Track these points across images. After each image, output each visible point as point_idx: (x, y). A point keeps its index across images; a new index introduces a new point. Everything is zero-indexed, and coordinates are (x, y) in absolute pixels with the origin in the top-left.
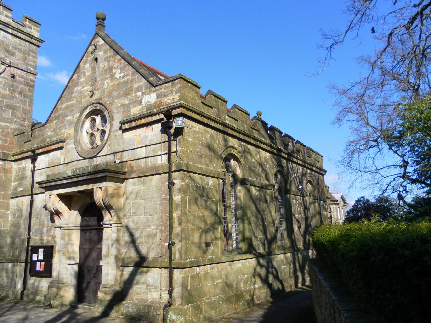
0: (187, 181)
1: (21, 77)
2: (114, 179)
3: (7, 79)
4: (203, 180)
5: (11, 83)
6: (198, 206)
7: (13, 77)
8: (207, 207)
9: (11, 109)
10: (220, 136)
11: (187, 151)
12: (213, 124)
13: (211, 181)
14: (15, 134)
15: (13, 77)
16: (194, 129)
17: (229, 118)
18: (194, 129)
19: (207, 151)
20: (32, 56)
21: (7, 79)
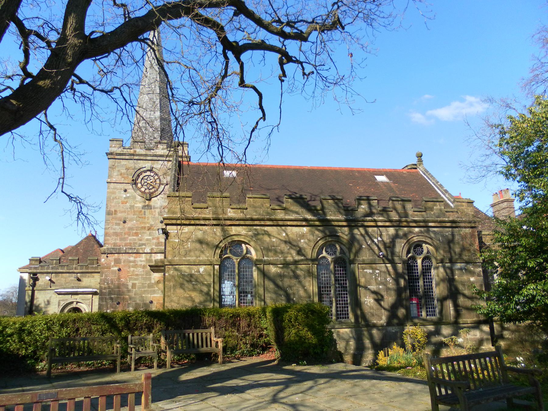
0: (172, 272)
2: (160, 271)
6: (184, 289)
8: (194, 290)
10: (218, 230)
13: (202, 269)
17: (232, 211)
19: (198, 245)
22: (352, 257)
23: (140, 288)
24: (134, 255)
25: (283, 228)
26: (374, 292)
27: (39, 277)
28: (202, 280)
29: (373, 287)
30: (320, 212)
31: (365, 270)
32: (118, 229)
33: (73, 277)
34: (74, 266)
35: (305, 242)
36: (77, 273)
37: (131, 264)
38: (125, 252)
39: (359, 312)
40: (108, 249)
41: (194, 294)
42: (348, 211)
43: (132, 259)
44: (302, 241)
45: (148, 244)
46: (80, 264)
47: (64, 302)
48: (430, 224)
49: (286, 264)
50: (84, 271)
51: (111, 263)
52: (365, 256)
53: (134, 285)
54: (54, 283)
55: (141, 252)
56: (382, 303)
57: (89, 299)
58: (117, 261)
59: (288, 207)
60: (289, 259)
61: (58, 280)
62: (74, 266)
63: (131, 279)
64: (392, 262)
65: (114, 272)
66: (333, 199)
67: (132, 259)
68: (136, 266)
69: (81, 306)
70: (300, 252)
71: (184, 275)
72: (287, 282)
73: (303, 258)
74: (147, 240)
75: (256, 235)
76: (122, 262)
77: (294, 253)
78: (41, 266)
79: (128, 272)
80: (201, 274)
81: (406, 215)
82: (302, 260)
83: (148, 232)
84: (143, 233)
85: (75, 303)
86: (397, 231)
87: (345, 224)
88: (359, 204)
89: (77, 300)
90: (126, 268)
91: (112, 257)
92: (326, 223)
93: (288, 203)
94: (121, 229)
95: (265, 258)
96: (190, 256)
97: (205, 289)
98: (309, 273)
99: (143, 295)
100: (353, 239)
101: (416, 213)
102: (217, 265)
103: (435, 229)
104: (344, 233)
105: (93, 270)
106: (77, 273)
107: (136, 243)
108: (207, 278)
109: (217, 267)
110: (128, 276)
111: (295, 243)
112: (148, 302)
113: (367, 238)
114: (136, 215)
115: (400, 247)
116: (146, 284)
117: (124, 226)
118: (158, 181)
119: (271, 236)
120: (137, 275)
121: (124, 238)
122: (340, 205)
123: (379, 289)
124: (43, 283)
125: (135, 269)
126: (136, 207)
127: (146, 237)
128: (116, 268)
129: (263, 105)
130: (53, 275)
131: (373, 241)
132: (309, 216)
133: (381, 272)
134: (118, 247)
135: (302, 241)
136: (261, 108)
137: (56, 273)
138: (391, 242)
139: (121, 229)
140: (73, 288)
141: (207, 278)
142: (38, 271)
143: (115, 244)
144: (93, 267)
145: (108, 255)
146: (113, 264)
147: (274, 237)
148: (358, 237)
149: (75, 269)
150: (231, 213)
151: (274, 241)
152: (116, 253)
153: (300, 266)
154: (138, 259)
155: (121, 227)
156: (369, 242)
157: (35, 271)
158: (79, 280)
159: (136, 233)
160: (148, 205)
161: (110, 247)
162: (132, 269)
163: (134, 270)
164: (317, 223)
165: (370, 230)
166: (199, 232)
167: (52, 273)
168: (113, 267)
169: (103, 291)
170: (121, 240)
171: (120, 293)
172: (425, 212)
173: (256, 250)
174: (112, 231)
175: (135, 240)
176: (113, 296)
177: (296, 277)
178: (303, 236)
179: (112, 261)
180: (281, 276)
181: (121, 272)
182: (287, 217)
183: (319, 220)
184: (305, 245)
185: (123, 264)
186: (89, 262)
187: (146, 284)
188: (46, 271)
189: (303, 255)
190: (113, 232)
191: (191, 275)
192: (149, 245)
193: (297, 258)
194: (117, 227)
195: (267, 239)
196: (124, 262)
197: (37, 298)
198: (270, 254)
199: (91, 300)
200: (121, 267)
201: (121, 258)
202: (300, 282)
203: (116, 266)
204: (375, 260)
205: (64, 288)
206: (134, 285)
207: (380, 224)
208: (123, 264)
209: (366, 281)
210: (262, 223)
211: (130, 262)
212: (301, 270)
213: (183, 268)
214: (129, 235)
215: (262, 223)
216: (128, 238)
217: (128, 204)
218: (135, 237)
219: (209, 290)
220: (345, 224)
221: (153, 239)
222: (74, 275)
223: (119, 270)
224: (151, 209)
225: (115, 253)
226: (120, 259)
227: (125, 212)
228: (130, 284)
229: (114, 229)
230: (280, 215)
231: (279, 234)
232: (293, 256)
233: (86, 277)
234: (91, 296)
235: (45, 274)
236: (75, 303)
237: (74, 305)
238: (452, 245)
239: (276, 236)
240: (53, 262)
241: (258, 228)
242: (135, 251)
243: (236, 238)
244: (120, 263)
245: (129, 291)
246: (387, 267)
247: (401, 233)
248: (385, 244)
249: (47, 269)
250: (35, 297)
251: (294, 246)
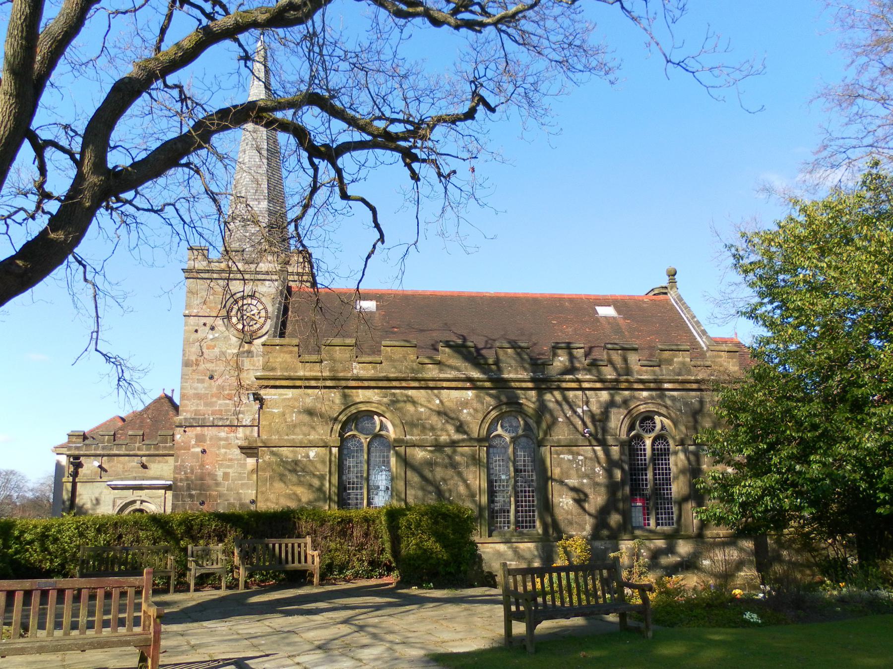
0: (268, 457)
4: (295, 453)
6: (285, 483)
8: (300, 483)
11: (270, 424)
12: (313, 383)
13: (312, 453)
16: (285, 397)
17: (358, 366)
18: (285, 397)
19: (306, 418)
22: (541, 435)
23: (236, 480)
24: (226, 428)
25: (436, 391)
26: (574, 489)
27: (83, 462)
28: (312, 469)
29: (573, 482)
30: (493, 367)
31: (562, 456)
32: (201, 388)
33: (134, 463)
34: (137, 445)
35: (469, 413)
36: (142, 456)
37: (222, 443)
38: (211, 424)
39: (549, 520)
40: (186, 419)
41: (299, 490)
42: (537, 365)
43: (223, 434)
44: (465, 411)
45: (247, 411)
46: (146, 442)
47: (121, 501)
48: (666, 386)
49: (438, 447)
50: (152, 452)
52: (561, 433)
53: (226, 476)
54: (106, 471)
56: (586, 506)
57: (160, 497)
58: (200, 439)
59: (444, 360)
60: (444, 438)
61: (112, 467)
62: (137, 445)
63: (221, 466)
64: (603, 443)
65: (194, 455)
66: (513, 347)
67: (223, 434)
68: (228, 446)
69: (147, 507)
70: (460, 428)
71: (287, 462)
72: (439, 473)
73: (465, 437)
75: (394, 402)
76: (208, 439)
77: (451, 429)
78: (86, 445)
79: (217, 455)
80: (310, 460)
81: (628, 371)
82: (463, 440)
85: (138, 502)
86: (612, 396)
87: (530, 385)
88: (555, 355)
89: (142, 498)
90: (214, 450)
91: (192, 433)
92: (500, 384)
93: (445, 355)
94: (206, 389)
95: (408, 437)
96: (294, 434)
97: (316, 483)
98: (475, 460)
99: (241, 491)
100: (542, 408)
101: (644, 368)
102: (336, 447)
103: (675, 393)
104: (529, 400)
105: (167, 452)
106: (142, 456)
107: (229, 411)
108: (319, 466)
109: (335, 450)
110: (217, 461)
111: (452, 415)
112: (248, 501)
113: (566, 407)
115: (617, 421)
116: (245, 473)
117: (210, 384)
118: (263, 313)
119: (418, 404)
120: (231, 460)
122: (526, 357)
123: (583, 484)
124: (89, 472)
125: (228, 451)
128: (199, 450)
129: (379, 221)
130: (105, 458)
131: (575, 412)
132: (476, 374)
133: (586, 458)
134: (201, 417)
135: (465, 411)
136: (377, 226)
137: (108, 455)
138: (602, 413)
140: (135, 479)
141: (319, 466)
142: (82, 452)
143: (196, 412)
144: (165, 447)
145: (187, 429)
146: (193, 442)
147: (422, 405)
148: (552, 405)
149: (139, 449)
150: (358, 370)
151: (422, 412)
152: (199, 426)
153: (459, 449)
155: (206, 385)
156: (569, 413)
157: (77, 452)
158: (144, 467)
159: (228, 395)
160: (249, 352)
161: (189, 416)
162: (223, 451)
163: (226, 453)
164: (488, 384)
165: (571, 394)
166: (310, 398)
167: (103, 456)
168: (193, 447)
169: (179, 484)
170: (206, 405)
171: (203, 488)
172: (659, 366)
173: (394, 425)
174: (192, 392)
175: (227, 405)
176: (194, 492)
177: (454, 465)
178: (465, 404)
179: (192, 438)
180: (430, 464)
181: (205, 456)
182: (442, 376)
183: (490, 380)
184: (469, 418)
185: (208, 442)
186: (159, 438)
187: (245, 473)
188: (93, 452)
189: (465, 433)
190: (194, 394)
191: (296, 462)
192: (249, 413)
193: (457, 437)
194: (199, 385)
195: (410, 408)
196: (211, 439)
197: (80, 495)
198: (415, 431)
199: (163, 498)
200: (205, 448)
201: (206, 433)
202: (460, 474)
203: (198, 446)
204: (577, 440)
205: (122, 479)
206: (226, 476)
207: (586, 385)
208: (208, 442)
209: (562, 473)
210: (404, 384)
211: (220, 439)
212: (462, 455)
213: (285, 451)
214: (219, 398)
215: (404, 384)
216: (216, 402)
217: (217, 350)
218: (228, 402)
219: (322, 485)
220: (530, 385)
222: (136, 458)
223: (204, 452)
224: (253, 357)
225: (196, 426)
226: (204, 435)
228: (220, 473)
229: (195, 389)
230: (432, 372)
231: (429, 402)
232: (450, 433)
233: (154, 462)
234: (163, 491)
235: (92, 458)
236: (138, 502)
237: (137, 506)
238: (699, 418)
239: (426, 403)
240: (104, 439)
241: (398, 391)
242: (228, 423)
243: (363, 408)
244: (204, 441)
245: (218, 484)
246: (594, 451)
247: (618, 399)
248: (593, 417)
249: (95, 450)
250: (77, 493)
251: (452, 419)
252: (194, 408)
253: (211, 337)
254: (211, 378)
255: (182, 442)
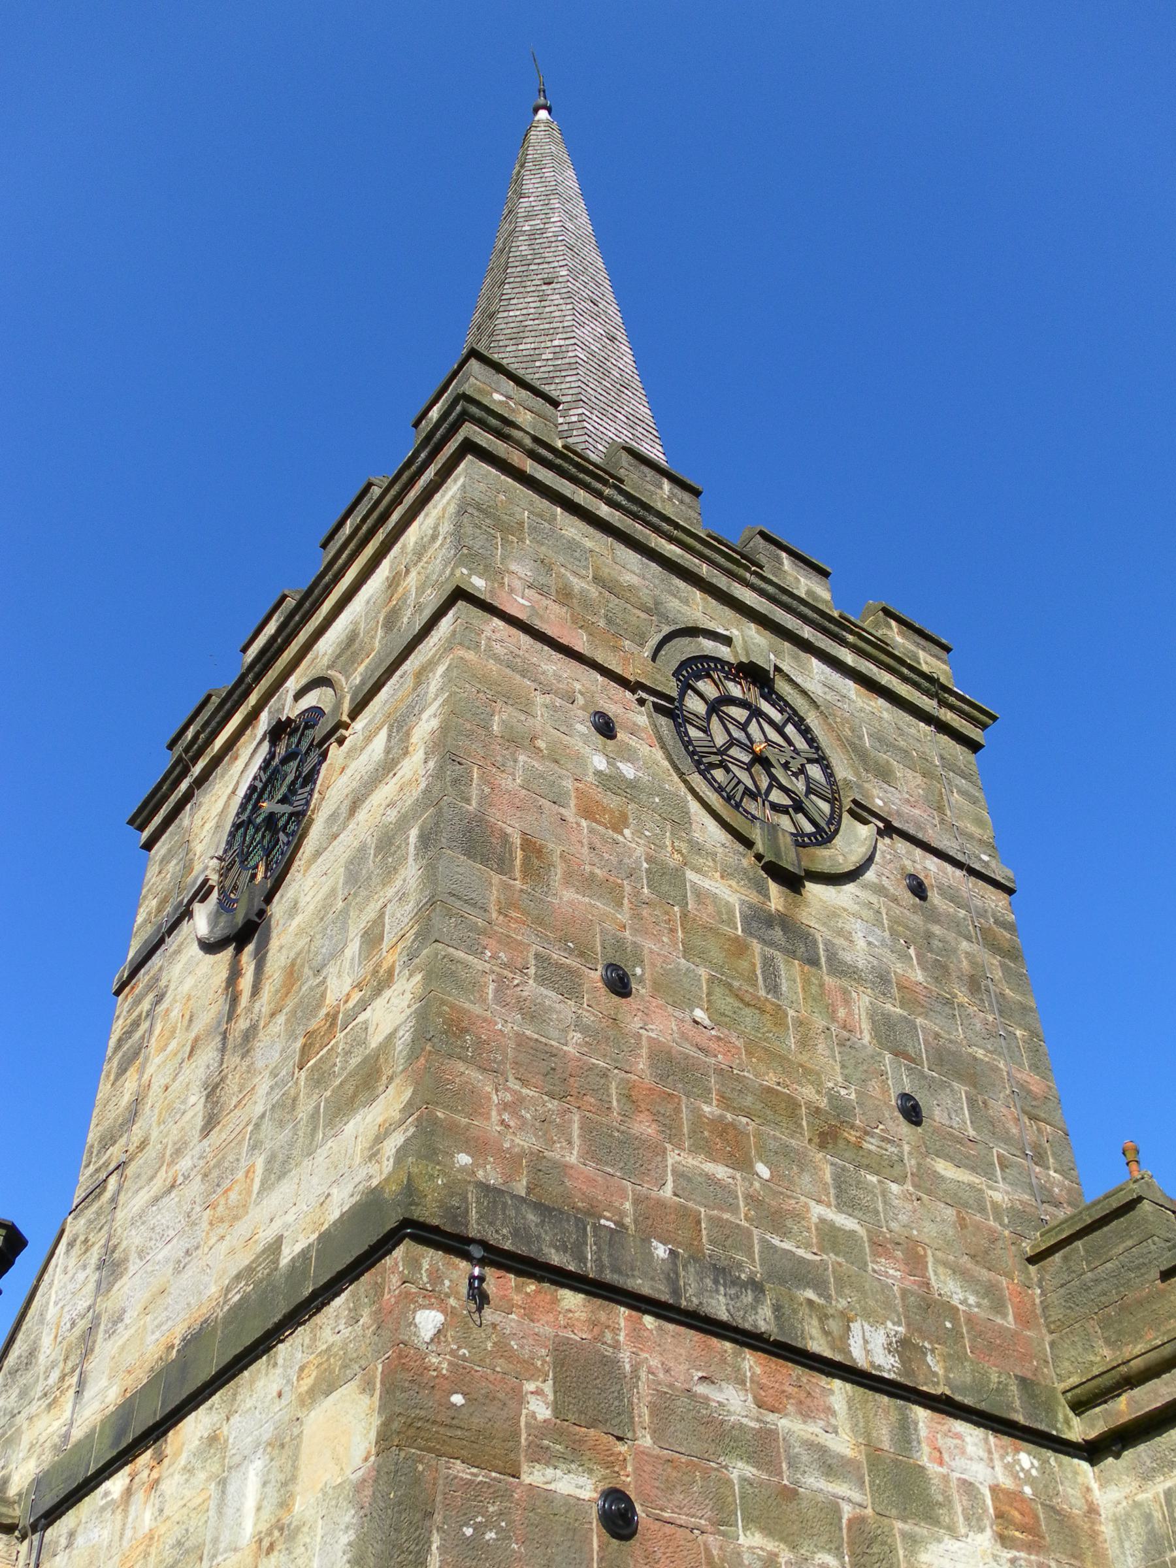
1: (945, 892)
3: (895, 900)
5: (917, 920)
7: (918, 889)
9: (960, 1077)
14: (1028, 1248)
15: (918, 889)
20: (960, 792)
21: (895, 900)
51: (520, 1398)
55: (818, 1346)
74: (831, 1237)
76: (643, 1414)
83: (825, 1166)
84: (785, 1151)
114: (702, 956)
121: (629, 1141)
126: (699, 894)
127: (817, 1211)
139: (595, 1038)
145: (497, 1282)
146: (540, 1409)
154: (788, 1424)
159: (722, 1129)
168: (540, 1455)
175: (722, 1195)
179: (528, 1369)
200: (628, 1481)
201: (625, 1357)
208: (646, 1441)
214: (671, 1131)
218: (721, 1172)
221: (879, 1246)
226: (610, 1365)
227: (614, 895)
242: (763, 1320)
252: (524, 1142)
253: (600, 762)
254: (619, 984)
255: (460, 1378)
